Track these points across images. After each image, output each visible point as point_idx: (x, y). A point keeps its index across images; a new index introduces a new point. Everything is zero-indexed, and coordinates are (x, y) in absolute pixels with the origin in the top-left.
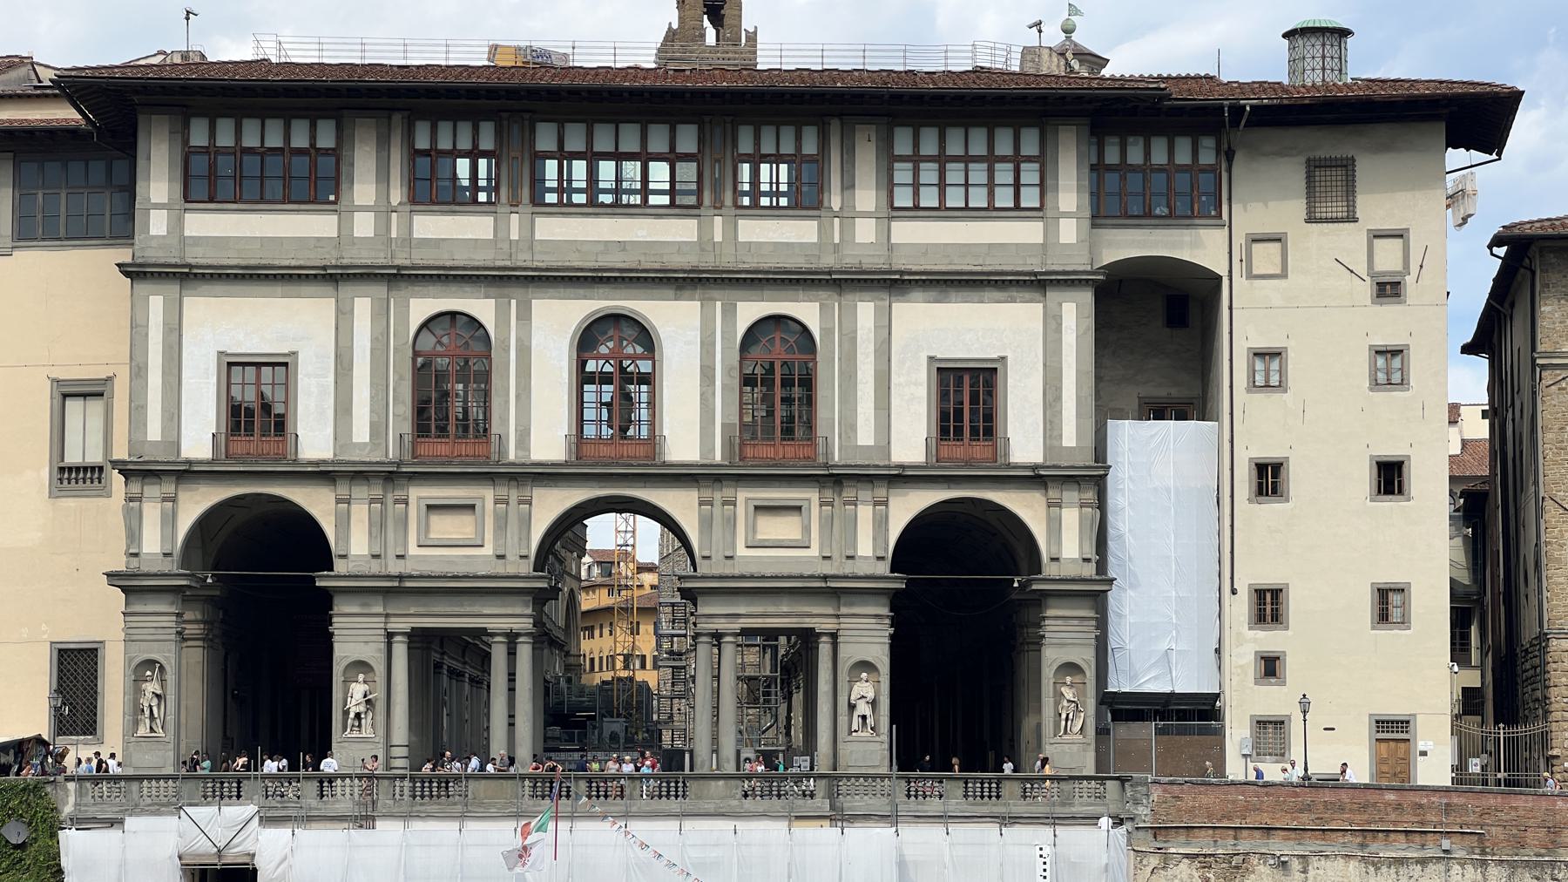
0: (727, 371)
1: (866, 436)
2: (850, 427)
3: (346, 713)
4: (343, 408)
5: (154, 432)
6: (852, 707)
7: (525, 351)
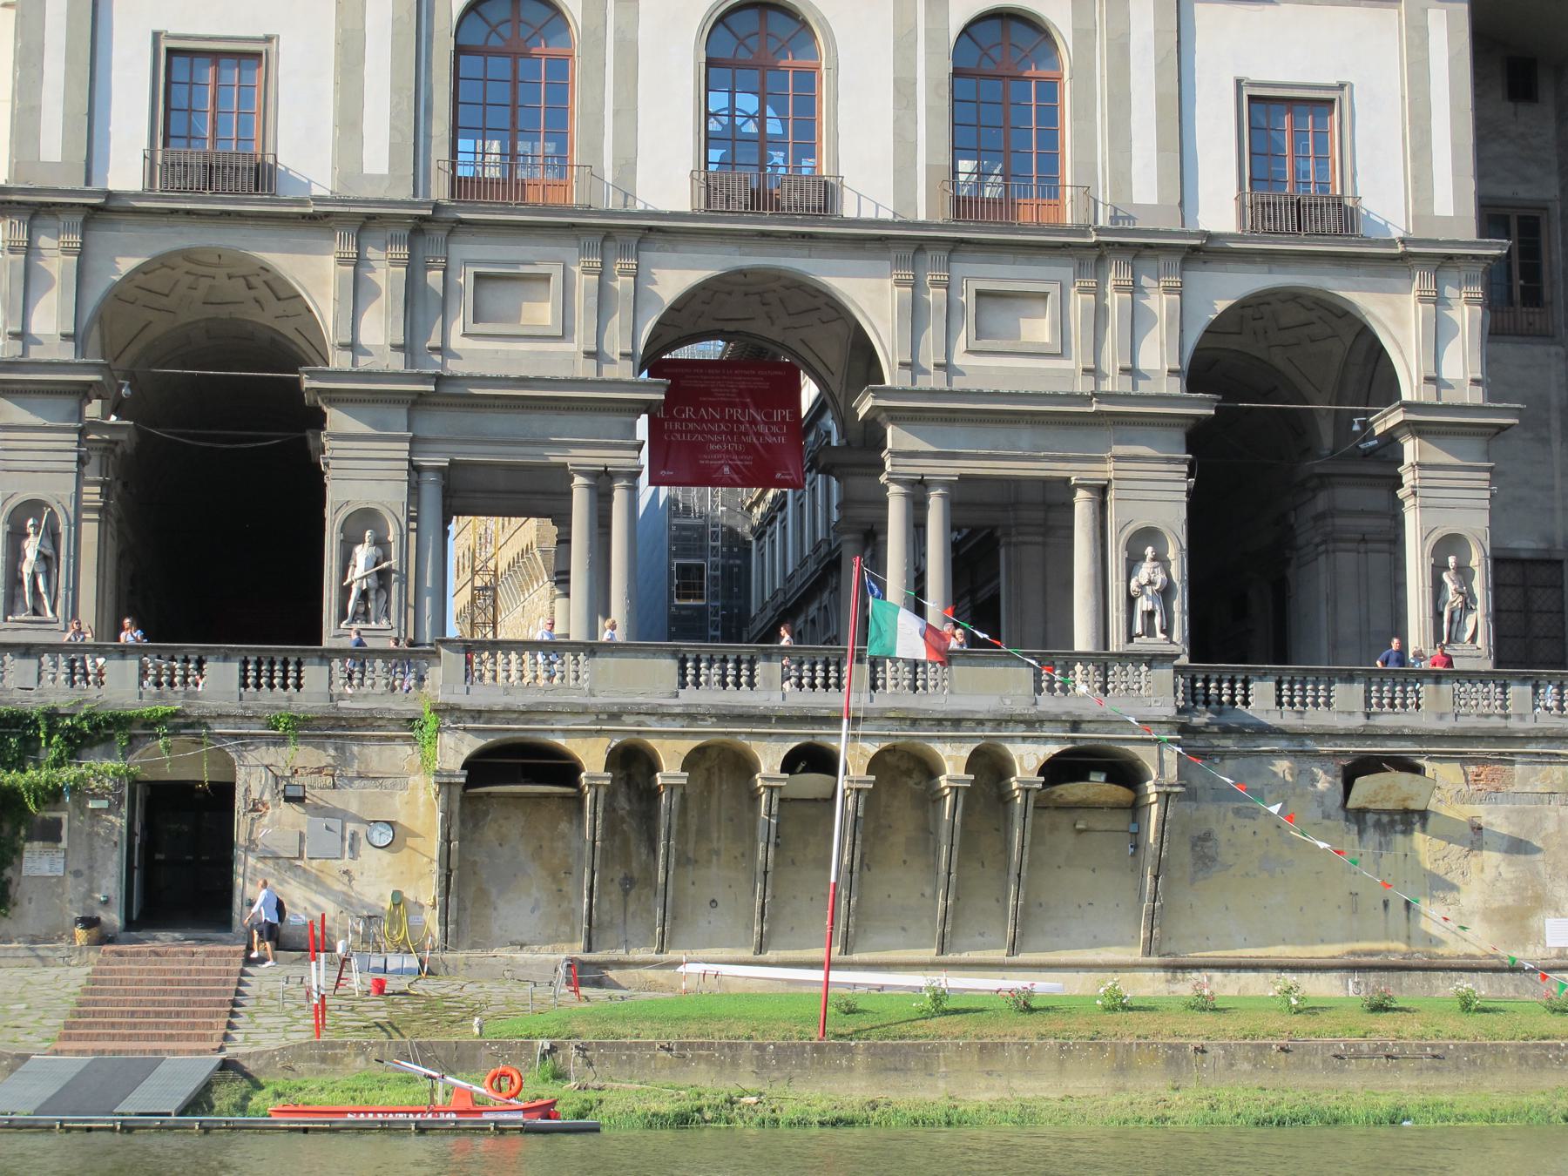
0: (932, 89)
1: (1147, 189)
2: (1121, 177)
3: (345, 591)
4: (349, 123)
5: (53, 145)
6: (1131, 601)
7: (628, 50)
